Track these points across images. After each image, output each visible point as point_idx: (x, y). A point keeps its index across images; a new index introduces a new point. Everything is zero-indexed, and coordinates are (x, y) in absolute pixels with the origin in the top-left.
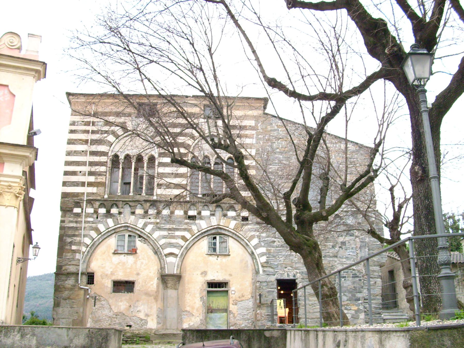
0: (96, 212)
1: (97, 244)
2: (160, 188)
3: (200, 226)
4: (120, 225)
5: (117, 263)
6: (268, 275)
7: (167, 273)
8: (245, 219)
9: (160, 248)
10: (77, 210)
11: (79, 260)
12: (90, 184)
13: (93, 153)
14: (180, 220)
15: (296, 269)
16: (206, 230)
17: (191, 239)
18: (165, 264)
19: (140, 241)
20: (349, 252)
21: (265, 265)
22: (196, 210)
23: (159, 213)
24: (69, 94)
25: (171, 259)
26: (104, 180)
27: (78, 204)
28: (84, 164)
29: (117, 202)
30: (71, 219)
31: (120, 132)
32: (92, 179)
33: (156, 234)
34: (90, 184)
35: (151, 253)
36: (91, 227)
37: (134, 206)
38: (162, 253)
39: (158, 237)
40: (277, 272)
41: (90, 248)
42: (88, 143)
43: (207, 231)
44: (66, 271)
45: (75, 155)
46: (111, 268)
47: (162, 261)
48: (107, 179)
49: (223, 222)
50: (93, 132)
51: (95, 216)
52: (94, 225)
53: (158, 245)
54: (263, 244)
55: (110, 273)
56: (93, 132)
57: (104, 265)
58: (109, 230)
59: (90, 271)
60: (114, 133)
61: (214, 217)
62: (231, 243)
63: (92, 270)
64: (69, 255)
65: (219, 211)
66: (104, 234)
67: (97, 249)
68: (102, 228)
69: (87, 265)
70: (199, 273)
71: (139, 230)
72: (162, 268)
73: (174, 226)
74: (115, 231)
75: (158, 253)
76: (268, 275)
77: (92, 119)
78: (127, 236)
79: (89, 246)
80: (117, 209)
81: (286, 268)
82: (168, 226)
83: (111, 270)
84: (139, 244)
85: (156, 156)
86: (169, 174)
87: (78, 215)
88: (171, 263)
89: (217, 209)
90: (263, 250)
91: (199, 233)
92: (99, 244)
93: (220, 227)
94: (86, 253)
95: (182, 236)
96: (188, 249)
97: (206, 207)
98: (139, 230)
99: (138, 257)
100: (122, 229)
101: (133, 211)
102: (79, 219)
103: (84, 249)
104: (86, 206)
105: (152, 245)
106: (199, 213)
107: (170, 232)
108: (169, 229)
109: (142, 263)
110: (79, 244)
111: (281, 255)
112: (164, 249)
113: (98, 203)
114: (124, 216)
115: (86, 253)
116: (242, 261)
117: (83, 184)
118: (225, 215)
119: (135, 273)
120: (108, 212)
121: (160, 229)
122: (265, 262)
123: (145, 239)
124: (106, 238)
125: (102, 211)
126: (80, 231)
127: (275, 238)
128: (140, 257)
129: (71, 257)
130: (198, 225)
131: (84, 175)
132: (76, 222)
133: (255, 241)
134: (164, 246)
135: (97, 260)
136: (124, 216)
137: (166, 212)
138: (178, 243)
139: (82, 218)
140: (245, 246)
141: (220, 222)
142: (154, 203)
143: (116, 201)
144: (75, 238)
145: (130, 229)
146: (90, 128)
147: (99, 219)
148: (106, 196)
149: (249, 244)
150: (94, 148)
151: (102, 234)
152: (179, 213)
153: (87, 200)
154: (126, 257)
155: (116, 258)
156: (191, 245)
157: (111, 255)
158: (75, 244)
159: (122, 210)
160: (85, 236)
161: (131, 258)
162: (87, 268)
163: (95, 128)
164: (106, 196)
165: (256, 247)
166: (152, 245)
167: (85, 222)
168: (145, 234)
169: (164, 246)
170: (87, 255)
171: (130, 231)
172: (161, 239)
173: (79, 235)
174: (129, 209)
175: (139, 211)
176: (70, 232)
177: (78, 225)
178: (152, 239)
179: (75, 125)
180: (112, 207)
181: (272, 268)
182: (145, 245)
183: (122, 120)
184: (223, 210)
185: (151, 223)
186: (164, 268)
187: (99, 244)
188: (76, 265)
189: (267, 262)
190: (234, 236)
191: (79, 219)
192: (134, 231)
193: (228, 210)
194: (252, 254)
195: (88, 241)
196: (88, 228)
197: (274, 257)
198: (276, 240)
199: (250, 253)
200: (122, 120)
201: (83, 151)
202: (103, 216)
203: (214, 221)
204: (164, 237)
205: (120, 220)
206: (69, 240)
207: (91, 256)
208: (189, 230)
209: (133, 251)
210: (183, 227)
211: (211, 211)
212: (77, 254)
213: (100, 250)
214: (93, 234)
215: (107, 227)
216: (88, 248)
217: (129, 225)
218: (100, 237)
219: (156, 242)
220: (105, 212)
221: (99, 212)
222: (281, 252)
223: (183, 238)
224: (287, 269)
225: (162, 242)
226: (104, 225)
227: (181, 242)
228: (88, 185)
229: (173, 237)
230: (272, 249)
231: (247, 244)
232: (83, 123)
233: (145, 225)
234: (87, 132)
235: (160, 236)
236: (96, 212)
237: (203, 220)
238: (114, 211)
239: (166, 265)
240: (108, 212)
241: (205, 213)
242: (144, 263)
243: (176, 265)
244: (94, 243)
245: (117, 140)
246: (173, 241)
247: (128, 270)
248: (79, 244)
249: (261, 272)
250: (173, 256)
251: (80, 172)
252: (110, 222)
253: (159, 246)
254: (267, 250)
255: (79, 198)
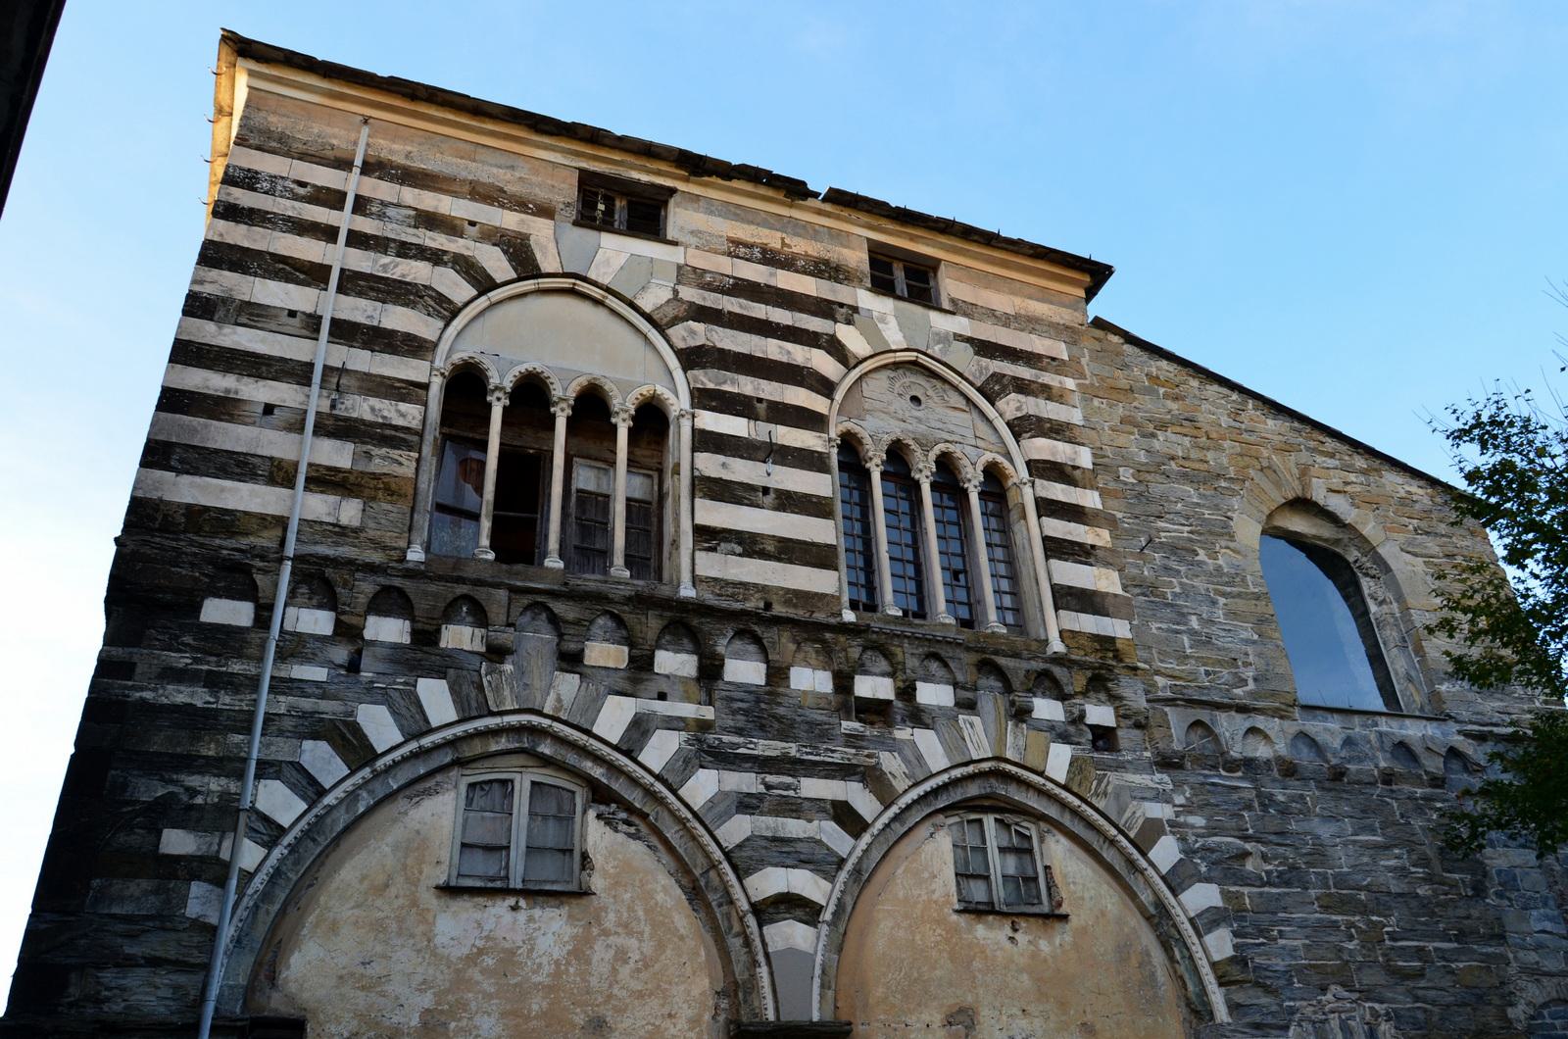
0: (348, 632)
1: (340, 826)
2: (713, 549)
3: (920, 758)
4: (492, 722)
5: (466, 951)
6: (1257, 1026)
7: (771, 1016)
8: (1103, 737)
9: (726, 867)
10: (224, 611)
11: (213, 931)
12: (324, 480)
13: (344, 332)
14: (818, 716)
15: (1368, 994)
16: (945, 778)
17: (879, 825)
18: (755, 963)
19: (608, 822)
20: (1539, 920)
21: (1235, 973)
22: (892, 675)
23: (710, 672)
24: (239, 47)
25: (789, 934)
26: (408, 470)
27: (238, 580)
28: (300, 373)
29: (480, 593)
30: (182, 660)
31: (496, 263)
32: (338, 454)
33: (703, 786)
34: (324, 480)
35: (667, 892)
36: (305, 715)
37: (577, 623)
38: (737, 893)
39: (712, 803)
40: (1292, 1011)
41: (293, 848)
42: (326, 281)
43: (945, 787)
44: (90, 1010)
45: (243, 320)
46: (424, 986)
47: (735, 943)
48: (424, 467)
49: (1015, 744)
50: (356, 239)
51: (341, 654)
52: (329, 708)
53: (713, 847)
54: (1203, 869)
55: (415, 1022)
56: (356, 239)
57: (376, 969)
58: (427, 741)
59: (276, 1004)
60: (468, 268)
61: (976, 720)
62: (1058, 853)
63: (291, 999)
64: (134, 896)
65: (991, 689)
66: (388, 769)
67: (334, 857)
68: (380, 726)
69: (258, 964)
70: (937, 1018)
71: (598, 759)
72: (735, 990)
73: (793, 749)
74: (458, 755)
75: (713, 898)
76: (1257, 1026)
77: (352, 183)
78: (527, 785)
79: (289, 839)
80: (480, 632)
81: (1324, 990)
82: (767, 747)
83: (427, 1000)
84: (597, 836)
85: (678, 402)
86: (751, 488)
87: (226, 638)
88: (792, 952)
89: (983, 682)
90: (1202, 896)
91: (914, 794)
92: (348, 829)
93: (1009, 767)
94: (258, 883)
95: (835, 804)
96: (861, 878)
97: (934, 666)
98: (598, 759)
99: (599, 921)
100: (503, 743)
101: (572, 646)
102: (236, 667)
103: (250, 855)
104: (292, 594)
105: (671, 849)
106: (907, 692)
107: (771, 779)
108: (763, 764)
109: (621, 956)
110: (226, 815)
111: (1288, 922)
112: (749, 872)
113: (367, 587)
114: (521, 671)
115: (258, 883)
116: (1123, 950)
117: (280, 474)
118: (1021, 714)
119: (580, 1019)
120: (425, 637)
121: (725, 759)
122: (1231, 960)
123: (629, 808)
124: (391, 796)
125: (388, 630)
126: (238, 738)
127: (1246, 838)
128: (610, 920)
129: (151, 905)
130: (908, 752)
131: (297, 427)
132: (215, 682)
133: (1166, 852)
134: (743, 860)
135: (334, 928)
136: (521, 671)
137: (744, 670)
138: (819, 842)
139: (261, 659)
140: (1123, 875)
141: (1001, 741)
142: (688, 623)
143: (479, 583)
144: (194, 781)
145: (546, 748)
146: (344, 220)
147: (366, 675)
148: (416, 555)
149: (1143, 863)
150: (359, 310)
151: (380, 764)
152: (810, 680)
153: (297, 559)
154: (522, 916)
155: (458, 926)
156: (876, 855)
157: (430, 900)
158: (187, 816)
159: (506, 637)
160: (268, 769)
161: (549, 930)
162: (250, 990)
163: (367, 225)
164: (416, 555)
165: (1176, 880)
166: (671, 849)
167: (281, 685)
168: (634, 781)
169: (743, 860)
170: (266, 896)
171: (546, 762)
172: (725, 816)
173: (232, 766)
174: (548, 636)
175: (605, 653)
176: (158, 743)
177: (226, 700)
178: (672, 813)
179: (255, 190)
180: (449, 615)
181: (1268, 990)
182: (637, 846)
183: (509, 220)
184: (1008, 688)
185: (672, 723)
186: (751, 986)
187: (348, 829)
188: (180, 966)
189: (1239, 960)
190: (1066, 820)
191: (236, 667)
192: (572, 758)
193: (1032, 691)
194: (1159, 918)
195: (279, 801)
196: (288, 723)
197: (1262, 932)
198: (1248, 846)
199: (1152, 910)
200: (509, 220)
201: (292, 314)
202: (393, 661)
203: (979, 737)
204: (747, 804)
205: (497, 690)
206: (150, 790)
207: (283, 911)
208: (874, 779)
209: (563, 885)
210: (836, 758)
211: (956, 685)
212: (197, 889)
213: (351, 873)
214: (321, 759)
215: (415, 728)
216: (278, 852)
217: (546, 722)
218: (367, 782)
219: (701, 830)
220: (406, 640)
221: (368, 634)
222: (1285, 909)
223: (846, 816)
224: (1329, 996)
225: (738, 829)
226: (394, 713)
227: (831, 834)
228: (308, 480)
229: (793, 808)
230: (1246, 890)
231: (1131, 863)
232: (301, 191)
233: (640, 729)
234: (329, 234)
235: (722, 795)
236: (348, 632)
237: (927, 727)
238: (459, 637)
239: (763, 971)
240: (425, 637)
241: (933, 694)
242: (635, 956)
243: (818, 971)
244: (319, 818)
245: (483, 302)
246: (794, 827)
247: (537, 1004)
248: (226, 815)
249: (1222, 1013)
250: (799, 913)
251: (269, 409)
252: (436, 698)
253: (718, 855)
254: (1225, 895)
255: (244, 542)
